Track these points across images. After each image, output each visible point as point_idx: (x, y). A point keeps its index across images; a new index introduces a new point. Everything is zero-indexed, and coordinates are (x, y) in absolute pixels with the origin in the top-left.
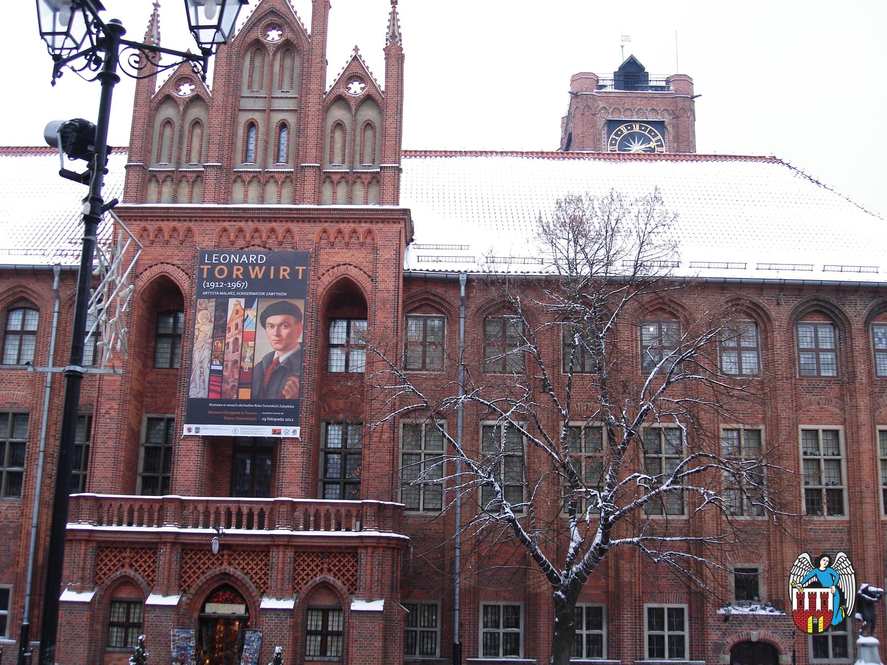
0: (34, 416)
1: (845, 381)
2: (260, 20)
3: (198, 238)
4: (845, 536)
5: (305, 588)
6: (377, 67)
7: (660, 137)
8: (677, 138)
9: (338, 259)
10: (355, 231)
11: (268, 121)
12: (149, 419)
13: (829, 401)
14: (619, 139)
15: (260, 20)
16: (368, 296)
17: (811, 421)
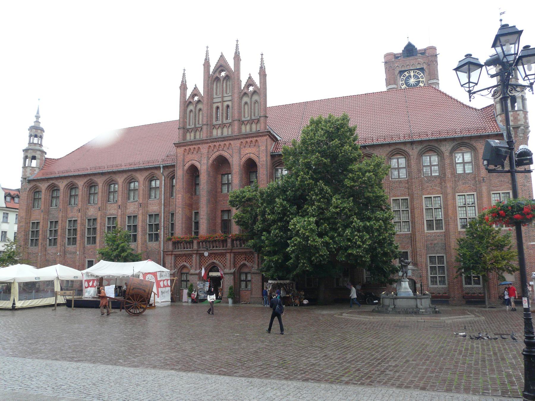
0: (160, 215)
1: (442, 177)
2: (217, 69)
3: (202, 150)
4: (443, 238)
5: (238, 266)
6: (257, 80)
7: (422, 74)
8: (429, 74)
9: (247, 152)
10: (252, 141)
11: (222, 106)
12: (195, 212)
13: (436, 186)
14: (404, 78)
15: (217, 69)
16: (258, 164)
17: (428, 194)
